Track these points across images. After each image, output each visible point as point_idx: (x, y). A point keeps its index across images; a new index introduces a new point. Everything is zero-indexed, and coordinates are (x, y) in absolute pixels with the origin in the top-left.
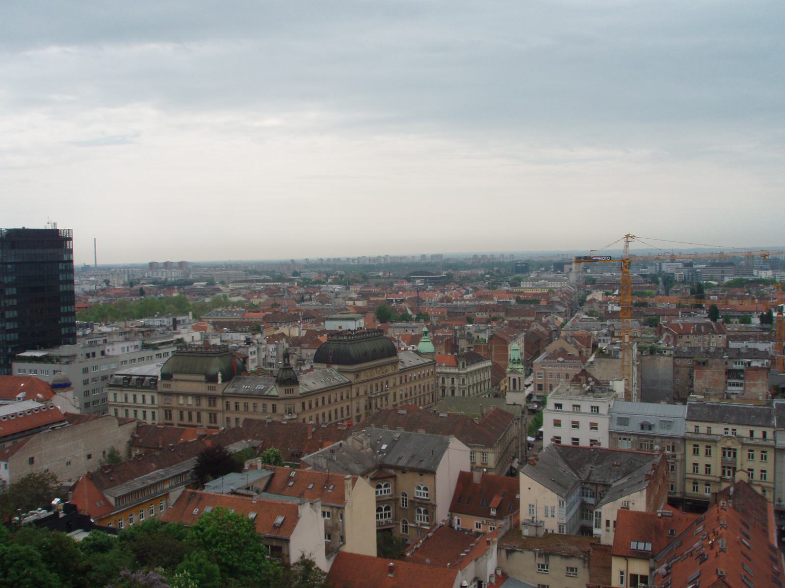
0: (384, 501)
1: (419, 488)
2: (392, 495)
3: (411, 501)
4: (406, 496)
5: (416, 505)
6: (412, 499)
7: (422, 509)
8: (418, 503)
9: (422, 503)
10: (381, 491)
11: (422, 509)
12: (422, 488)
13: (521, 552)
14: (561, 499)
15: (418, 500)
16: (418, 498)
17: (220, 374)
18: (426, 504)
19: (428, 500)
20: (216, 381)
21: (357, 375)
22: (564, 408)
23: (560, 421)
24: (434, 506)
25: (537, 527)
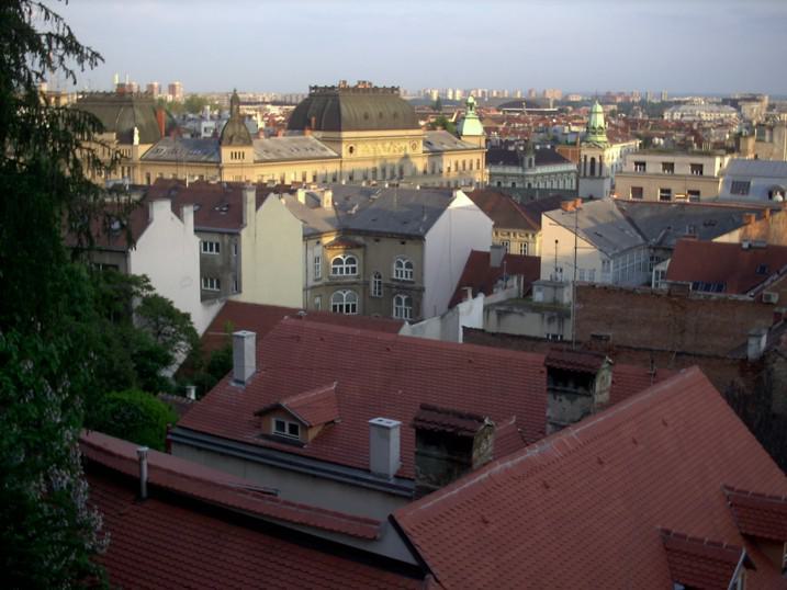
0: (346, 284)
1: (400, 265)
2: (358, 277)
3: (387, 286)
4: (380, 277)
5: (395, 290)
6: (389, 282)
7: (403, 298)
8: (397, 287)
9: (404, 288)
10: (342, 269)
11: (403, 298)
12: (404, 263)
13: (521, 314)
14: (605, 257)
15: (396, 283)
16: (398, 280)
17: (136, 131)
18: (411, 289)
19: (412, 282)
20: (132, 141)
21: (351, 148)
22: (650, 169)
23: (641, 189)
24: (422, 290)
25: (555, 287)
